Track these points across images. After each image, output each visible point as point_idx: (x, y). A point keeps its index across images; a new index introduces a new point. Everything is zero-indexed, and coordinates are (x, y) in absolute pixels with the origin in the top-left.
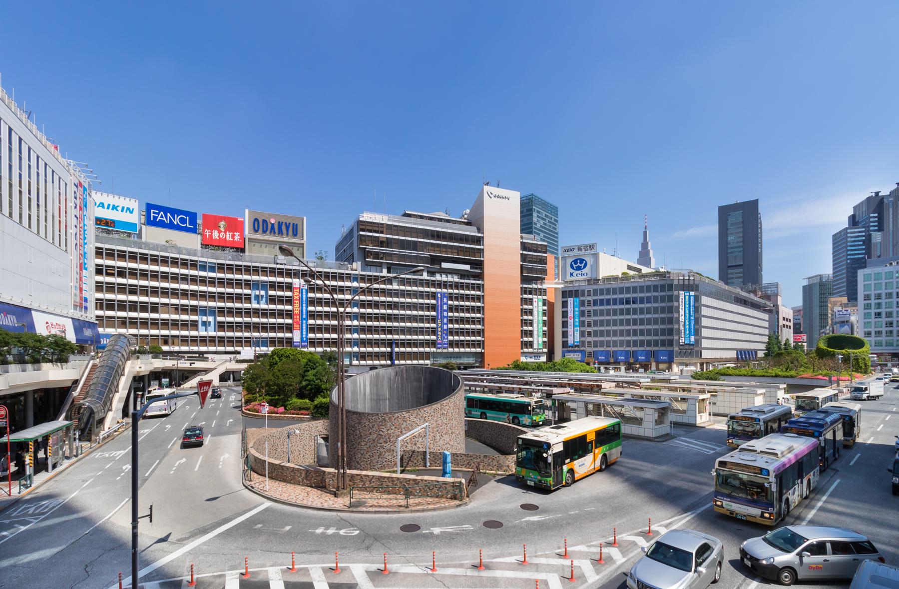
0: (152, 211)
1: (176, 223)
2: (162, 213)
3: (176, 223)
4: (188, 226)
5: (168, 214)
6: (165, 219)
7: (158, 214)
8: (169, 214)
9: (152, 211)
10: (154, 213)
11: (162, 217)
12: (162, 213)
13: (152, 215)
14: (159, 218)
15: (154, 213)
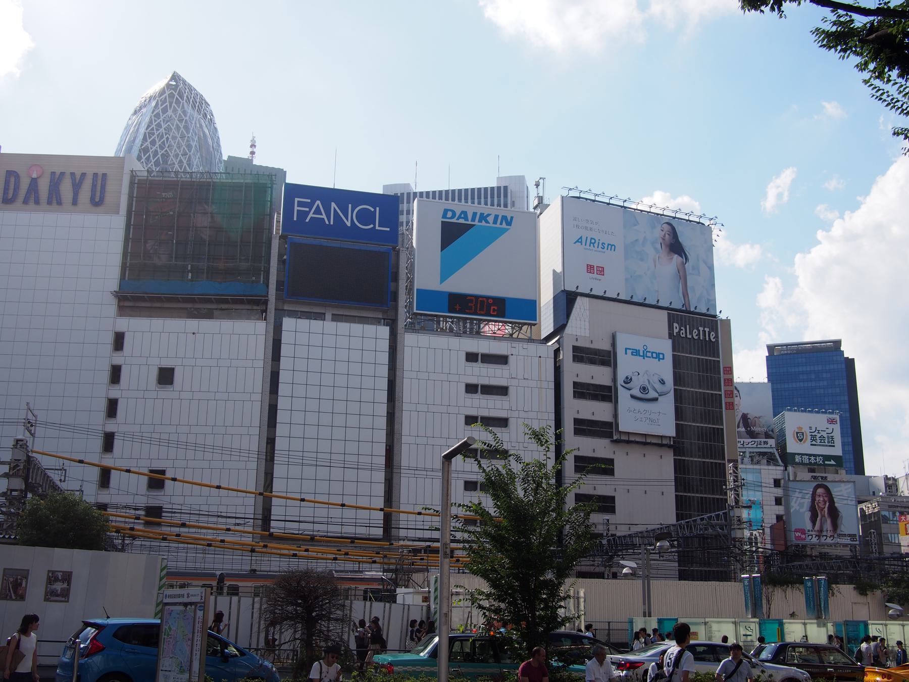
0: (297, 200)
1: (349, 224)
2: (318, 202)
3: (349, 224)
4: (377, 228)
5: (333, 205)
6: (324, 216)
7: (310, 206)
8: (333, 205)
9: (297, 200)
10: (300, 204)
11: (318, 211)
12: (318, 202)
13: (296, 208)
14: (311, 215)
15: (300, 204)
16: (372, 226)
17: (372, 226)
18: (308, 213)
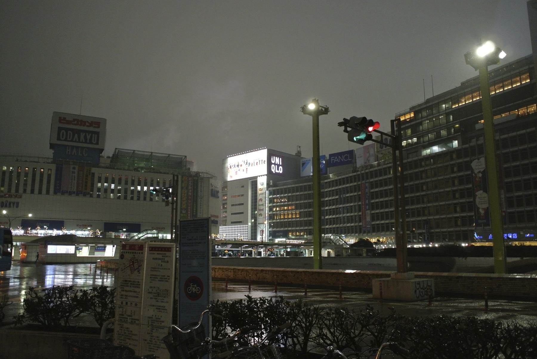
1: (343, 160)
2: (336, 157)
3: (343, 160)
5: (339, 157)
6: (338, 160)
7: (334, 158)
8: (339, 157)
10: (333, 159)
11: (336, 159)
12: (336, 157)
13: (332, 160)
14: (335, 161)
15: (333, 159)
16: (347, 160)
17: (347, 160)
18: (334, 160)
